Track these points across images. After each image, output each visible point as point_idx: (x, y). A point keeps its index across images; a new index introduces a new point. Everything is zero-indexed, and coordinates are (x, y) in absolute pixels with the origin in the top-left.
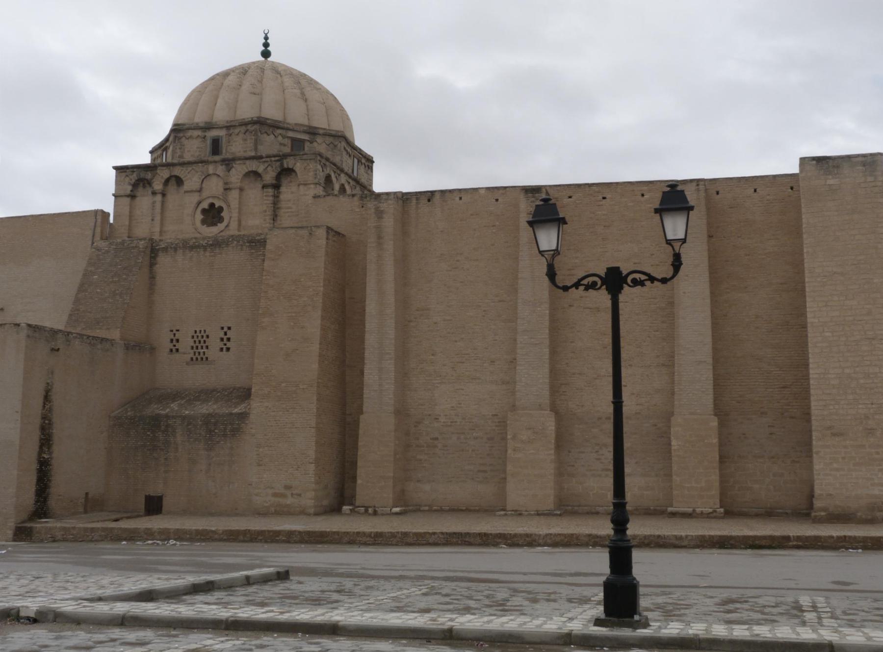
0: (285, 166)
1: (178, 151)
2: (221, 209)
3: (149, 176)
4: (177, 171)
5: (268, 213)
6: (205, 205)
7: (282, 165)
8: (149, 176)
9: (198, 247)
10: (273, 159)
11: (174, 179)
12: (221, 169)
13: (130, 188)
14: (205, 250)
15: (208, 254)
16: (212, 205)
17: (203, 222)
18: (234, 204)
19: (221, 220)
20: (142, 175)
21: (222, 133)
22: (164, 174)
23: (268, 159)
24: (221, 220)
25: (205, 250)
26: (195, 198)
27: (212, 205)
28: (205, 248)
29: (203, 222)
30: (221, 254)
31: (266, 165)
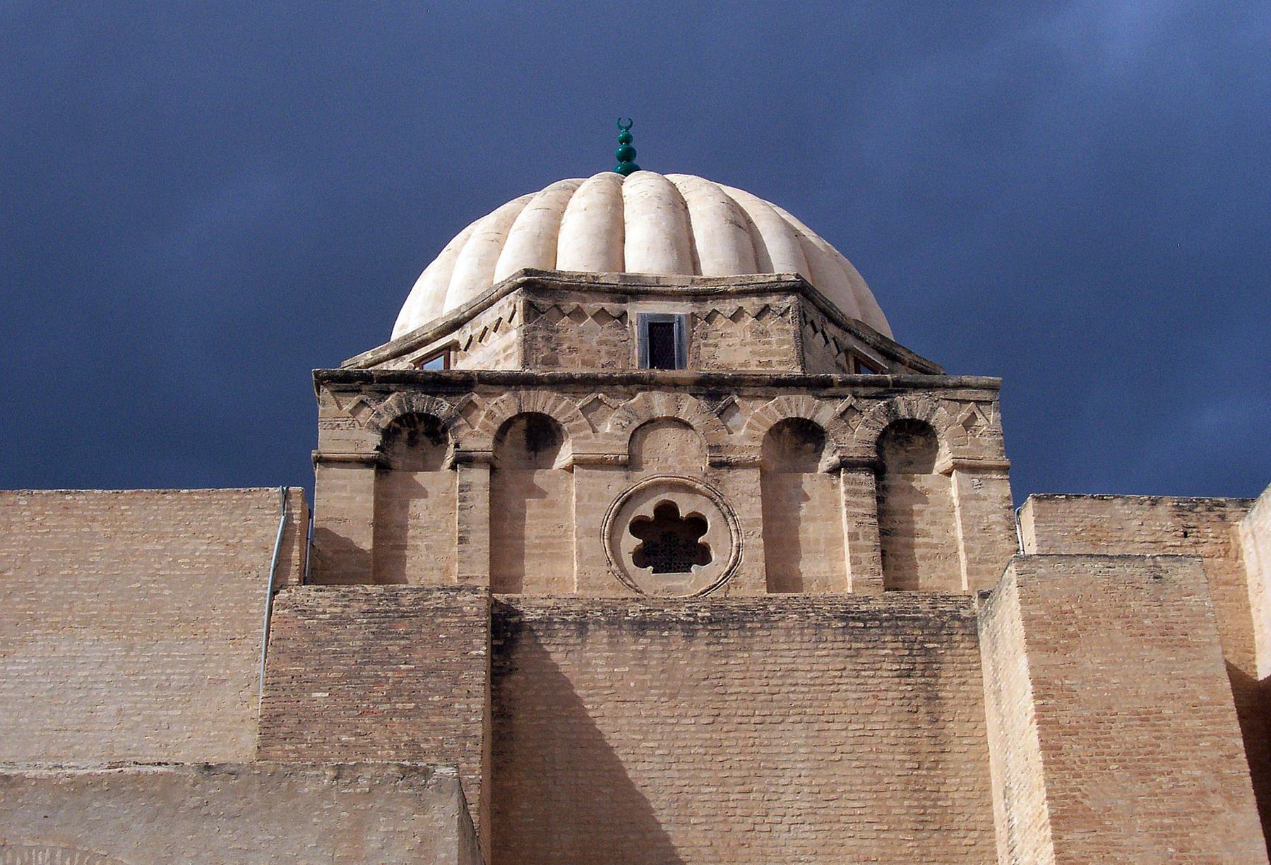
0: (903, 413)
1: (540, 343)
2: (698, 524)
3: (443, 407)
4: (542, 402)
5: (861, 542)
6: (647, 509)
7: (891, 409)
8: (443, 407)
9: (663, 624)
10: (862, 391)
11: (523, 423)
12: (689, 407)
13: (375, 439)
14: (690, 635)
15: (699, 646)
16: (667, 511)
17: (641, 558)
18: (750, 508)
19: (703, 556)
20: (420, 403)
21: (681, 309)
22: (504, 405)
23: (847, 390)
24: (703, 556)
25: (690, 635)
26: (615, 484)
27: (667, 511)
28: (689, 628)
29: (641, 558)
30: (748, 649)
31: (841, 406)
